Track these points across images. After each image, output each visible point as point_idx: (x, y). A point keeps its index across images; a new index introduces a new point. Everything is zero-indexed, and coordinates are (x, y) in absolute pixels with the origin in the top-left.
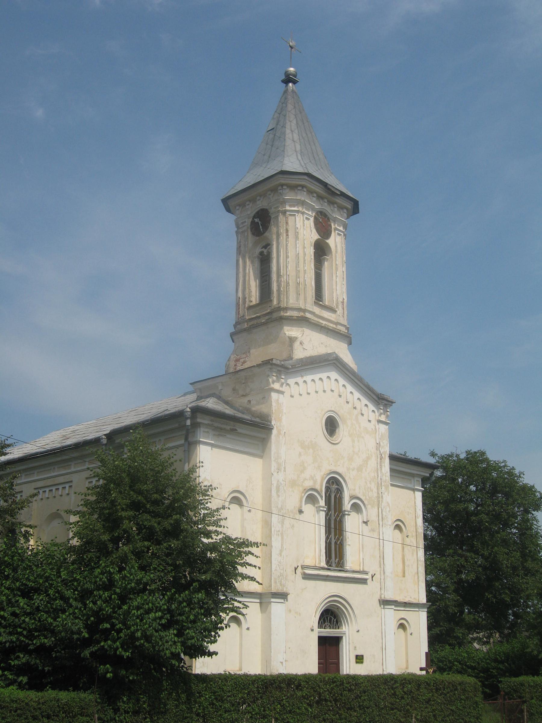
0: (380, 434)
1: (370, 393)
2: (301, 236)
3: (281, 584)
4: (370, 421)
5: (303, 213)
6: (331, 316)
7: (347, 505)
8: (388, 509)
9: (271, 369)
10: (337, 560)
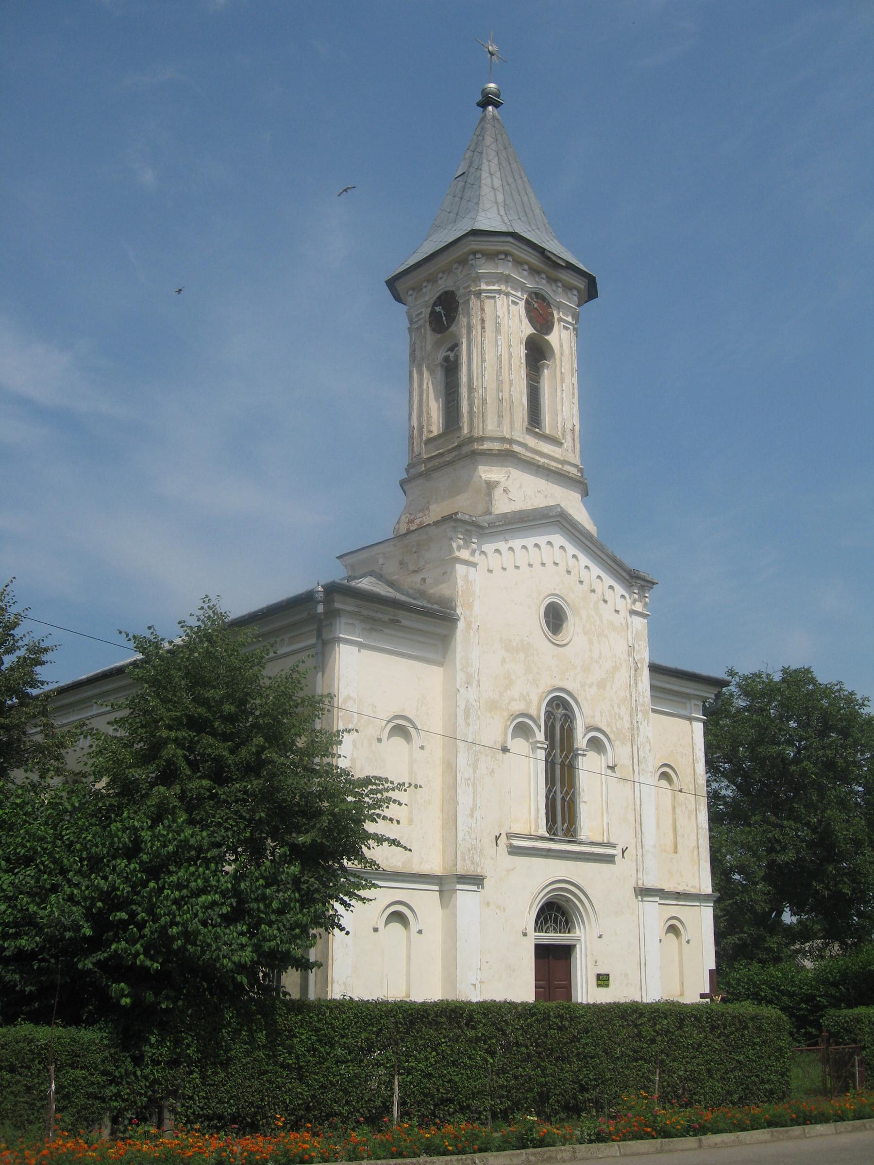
0: (634, 632)
1: (616, 567)
2: (504, 329)
3: (472, 863)
4: (617, 612)
5: (507, 294)
6: (554, 451)
7: (581, 740)
8: (648, 748)
9: (455, 527)
10: (566, 825)
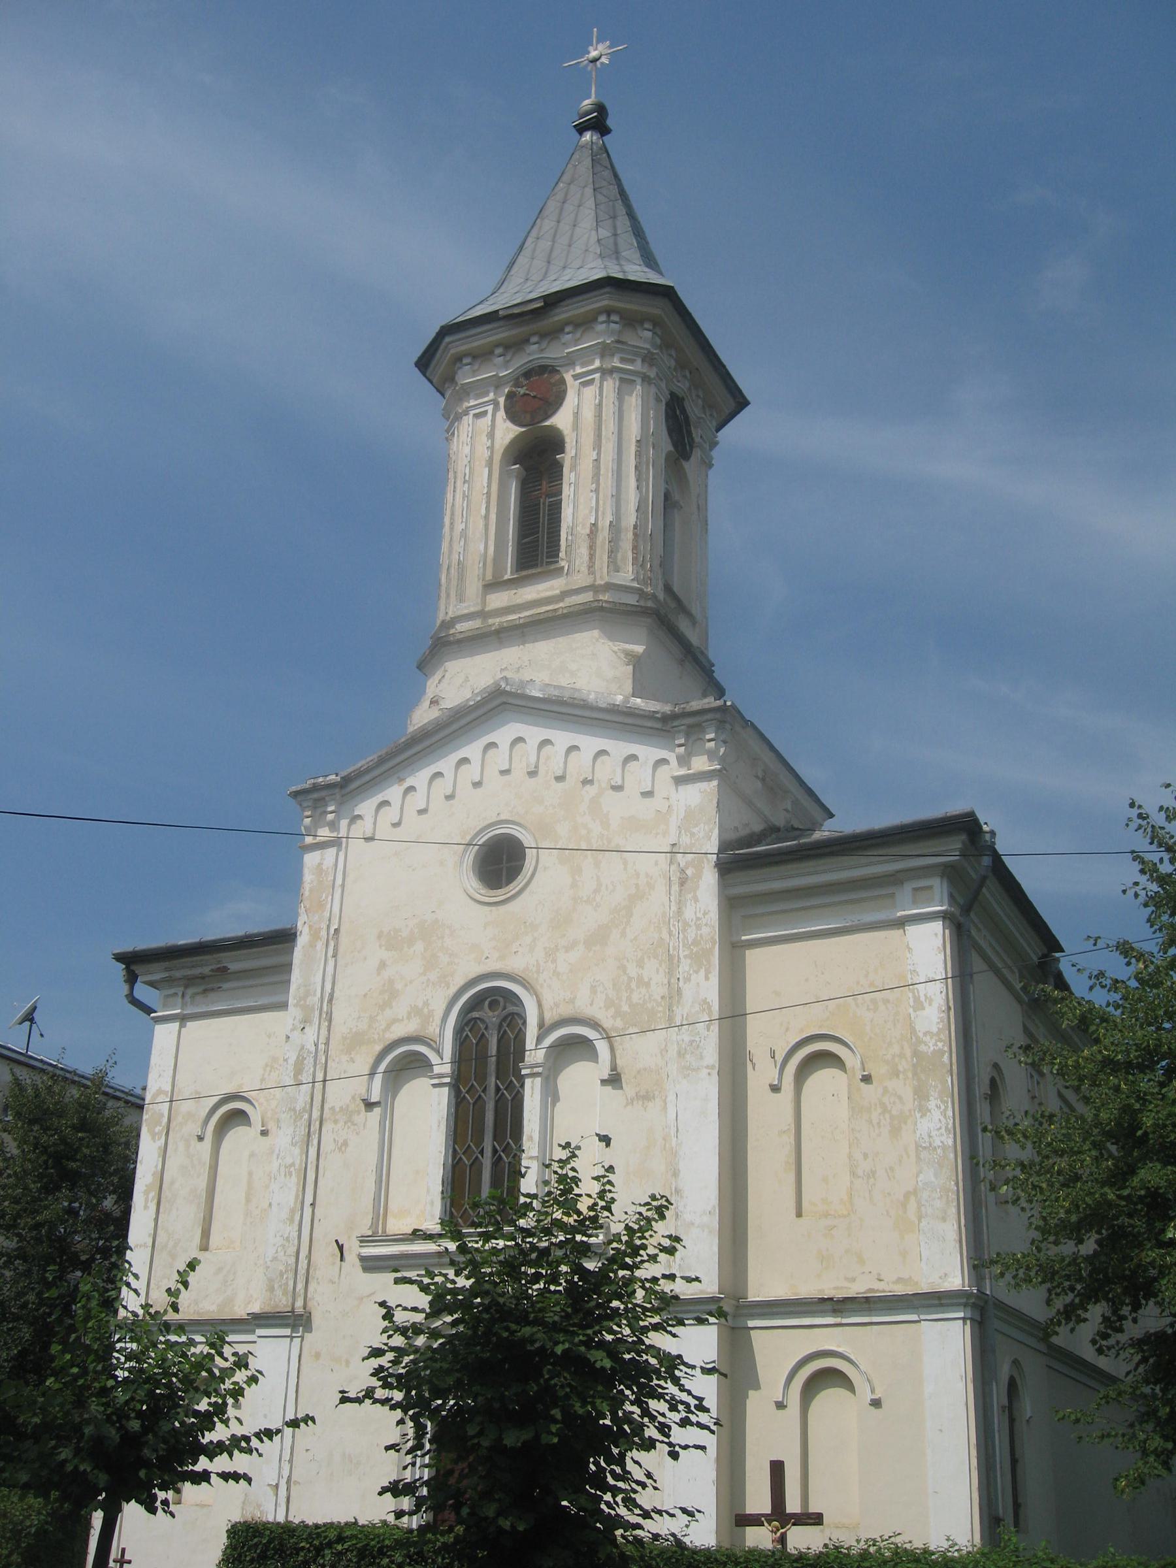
6: (552, 588)
